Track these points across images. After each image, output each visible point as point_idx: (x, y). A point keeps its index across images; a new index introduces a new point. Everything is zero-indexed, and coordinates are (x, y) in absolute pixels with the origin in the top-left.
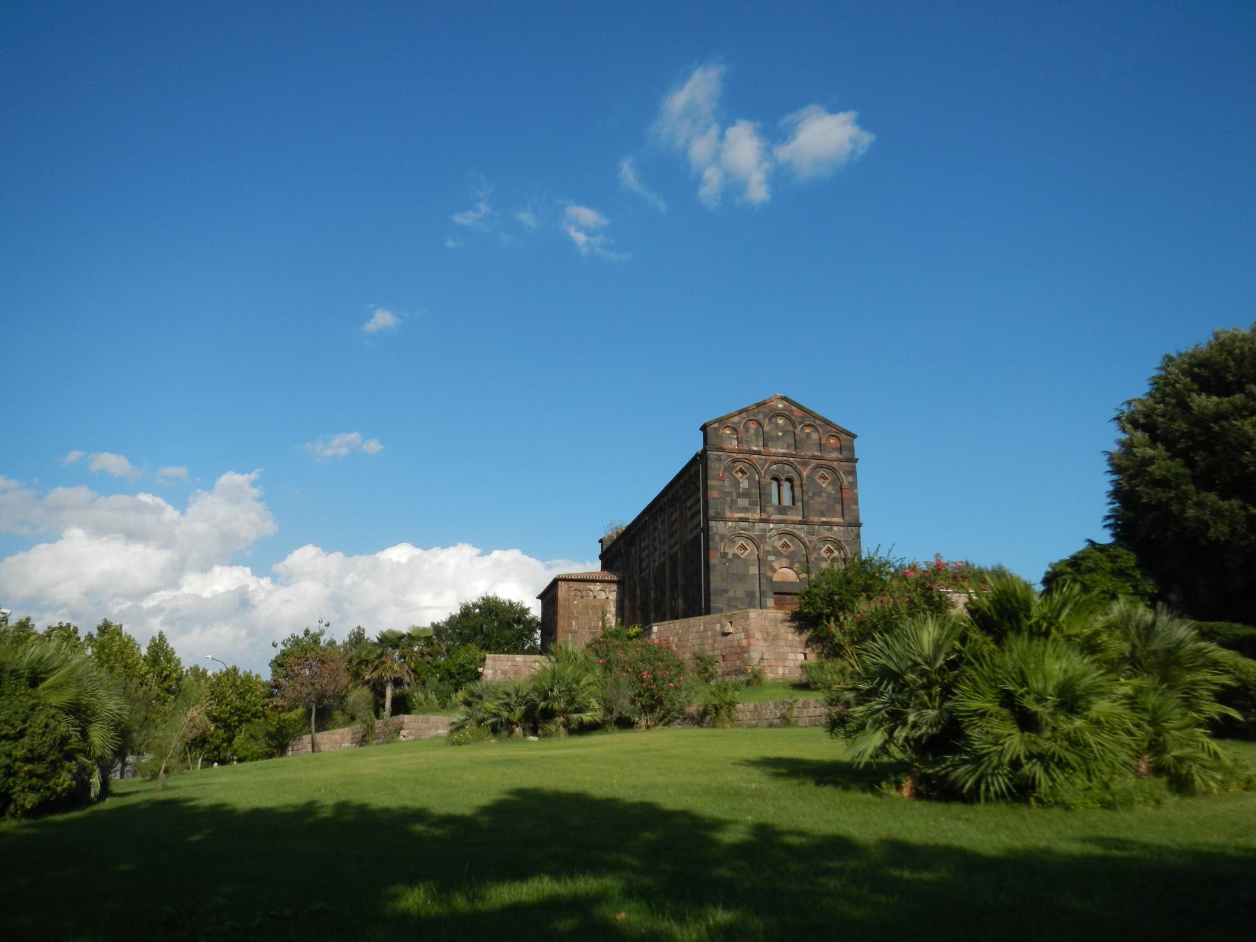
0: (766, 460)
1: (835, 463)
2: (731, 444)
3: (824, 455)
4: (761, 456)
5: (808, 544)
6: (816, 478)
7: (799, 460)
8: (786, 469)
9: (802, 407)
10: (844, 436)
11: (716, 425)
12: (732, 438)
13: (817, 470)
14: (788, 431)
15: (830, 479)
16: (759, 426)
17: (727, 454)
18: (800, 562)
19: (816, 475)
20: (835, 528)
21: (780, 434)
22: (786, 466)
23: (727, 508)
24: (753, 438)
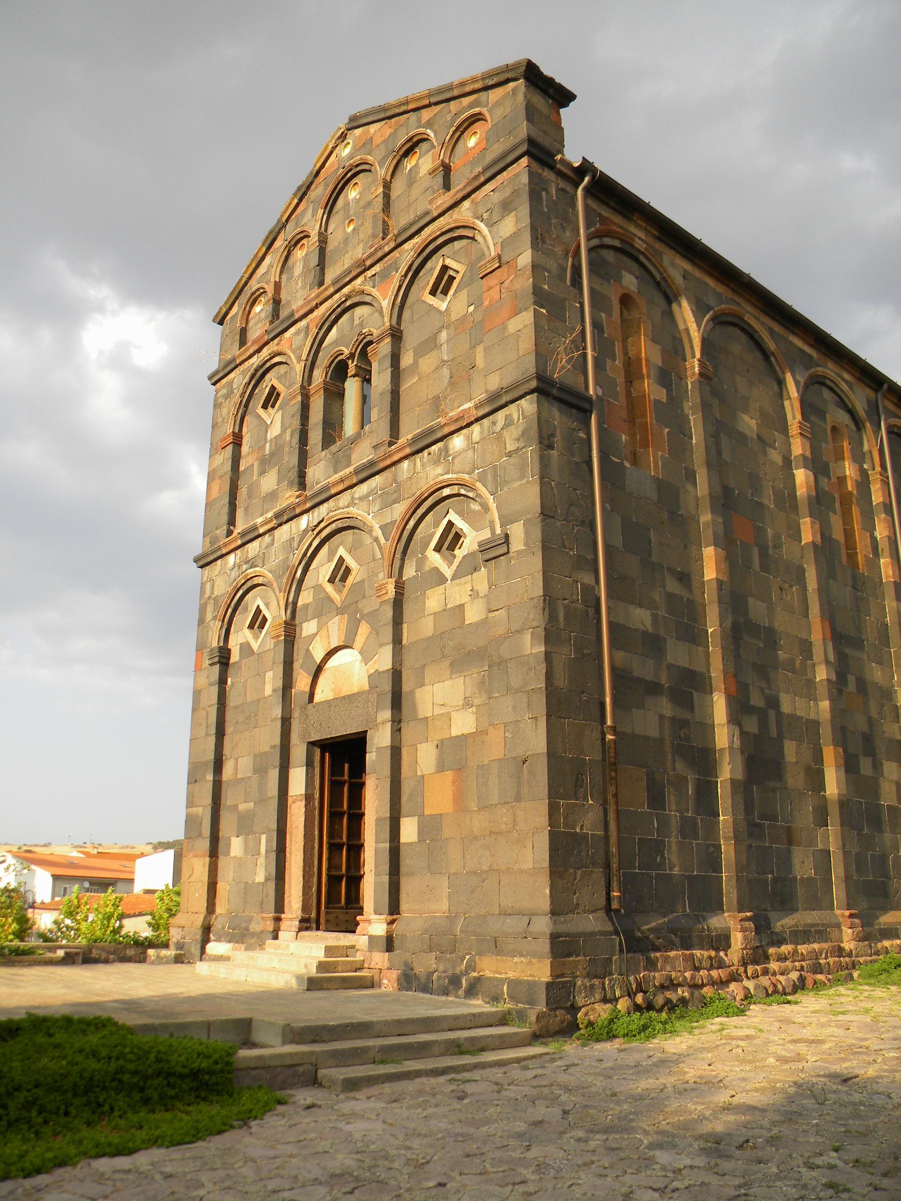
0: (308, 327)
5: (382, 540)
9: (384, 109)
18: (371, 617)
19: (424, 288)
20: (458, 442)
21: (350, 229)
23: (240, 513)
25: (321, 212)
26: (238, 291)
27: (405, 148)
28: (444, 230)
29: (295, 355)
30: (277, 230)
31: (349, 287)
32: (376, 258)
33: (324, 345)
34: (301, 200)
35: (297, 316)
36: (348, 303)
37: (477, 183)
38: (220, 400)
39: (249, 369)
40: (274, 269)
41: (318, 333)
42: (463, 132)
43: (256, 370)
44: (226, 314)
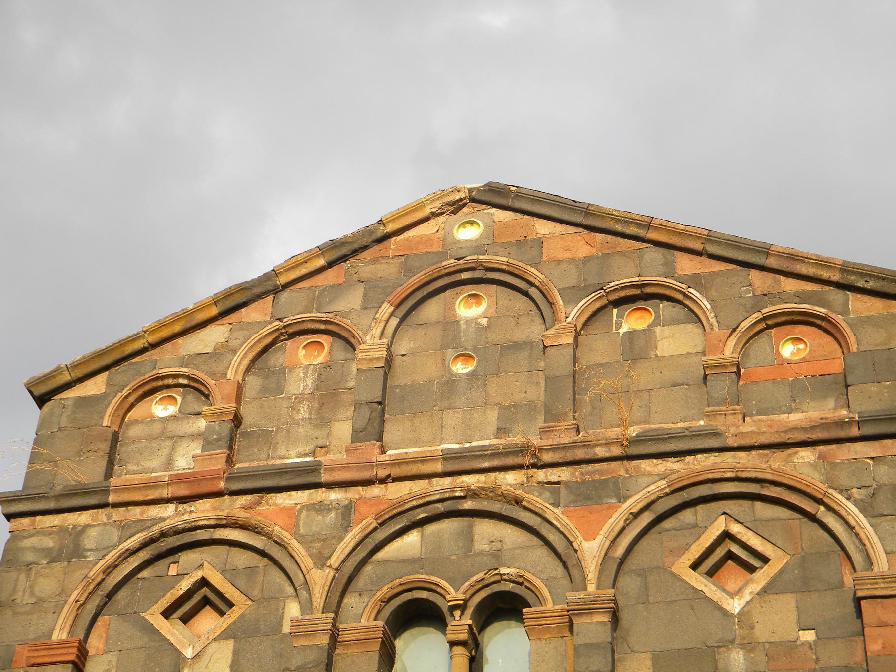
0: (347, 512)
1: (806, 455)
2: (169, 463)
3: (719, 424)
4: (320, 495)
6: (682, 566)
7: (564, 474)
8: (481, 545)
9: (587, 210)
10: (860, 305)
11: (95, 387)
12: (176, 438)
13: (687, 516)
14: (516, 347)
15: (779, 560)
16: (341, 354)
17: (118, 514)
22: (485, 529)
24: (304, 412)
25: (386, 309)
26: (117, 356)
27: (623, 294)
28: (744, 475)
29: (307, 549)
30: (257, 291)
31: (482, 477)
32: (570, 456)
33: (381, 555)
34: (330, 265)
35: (324, 477)
36: (468, 505)
37: (842, 434)
38: (30, 557)
39: (142, 525)
40: (237, 359)
41: (375, 529)
42: (769, 327)
43: (163, 534)
44: (68, 386)
